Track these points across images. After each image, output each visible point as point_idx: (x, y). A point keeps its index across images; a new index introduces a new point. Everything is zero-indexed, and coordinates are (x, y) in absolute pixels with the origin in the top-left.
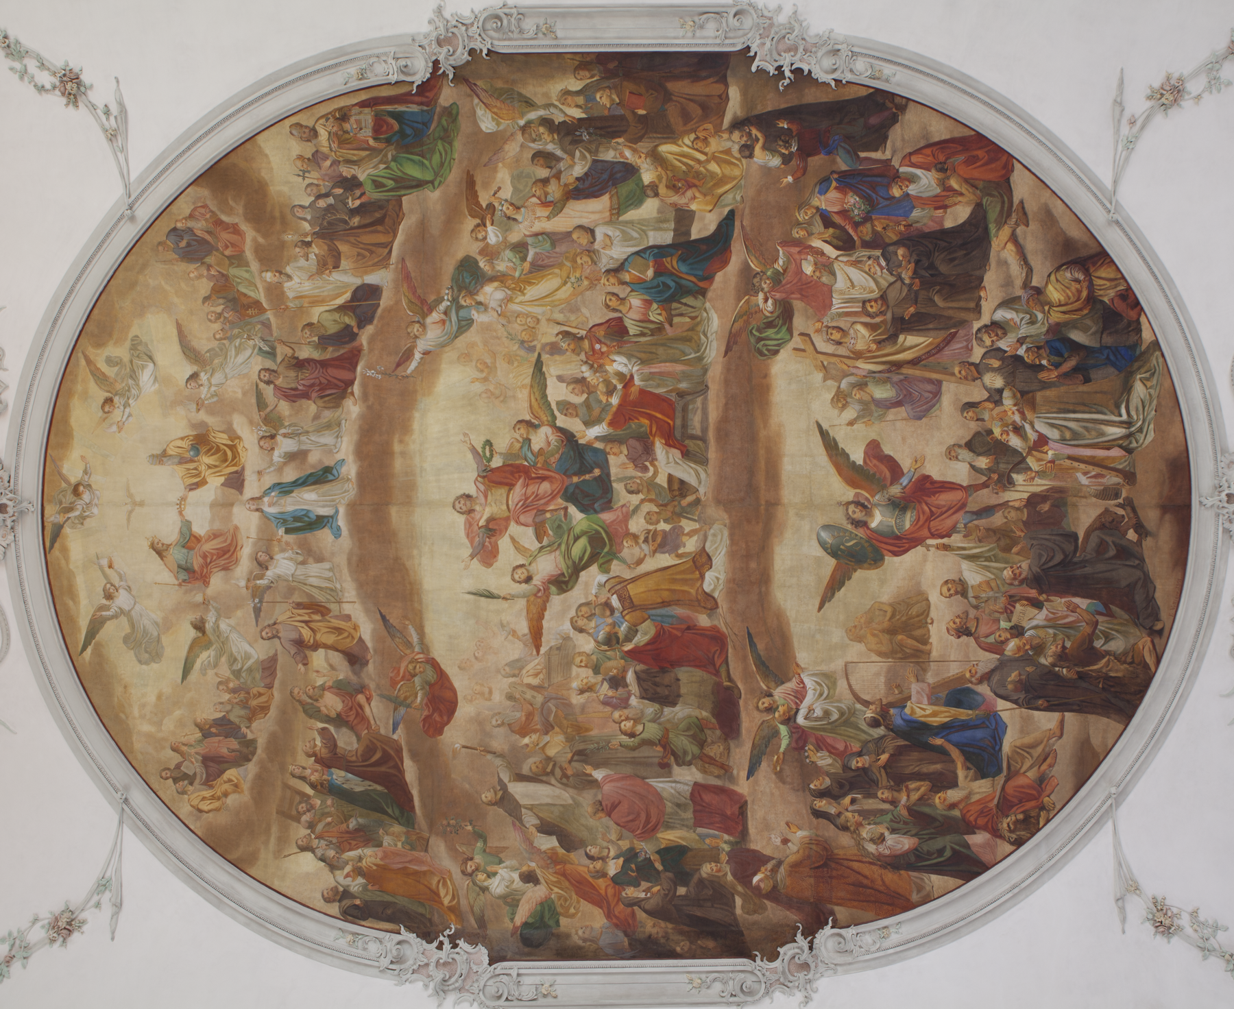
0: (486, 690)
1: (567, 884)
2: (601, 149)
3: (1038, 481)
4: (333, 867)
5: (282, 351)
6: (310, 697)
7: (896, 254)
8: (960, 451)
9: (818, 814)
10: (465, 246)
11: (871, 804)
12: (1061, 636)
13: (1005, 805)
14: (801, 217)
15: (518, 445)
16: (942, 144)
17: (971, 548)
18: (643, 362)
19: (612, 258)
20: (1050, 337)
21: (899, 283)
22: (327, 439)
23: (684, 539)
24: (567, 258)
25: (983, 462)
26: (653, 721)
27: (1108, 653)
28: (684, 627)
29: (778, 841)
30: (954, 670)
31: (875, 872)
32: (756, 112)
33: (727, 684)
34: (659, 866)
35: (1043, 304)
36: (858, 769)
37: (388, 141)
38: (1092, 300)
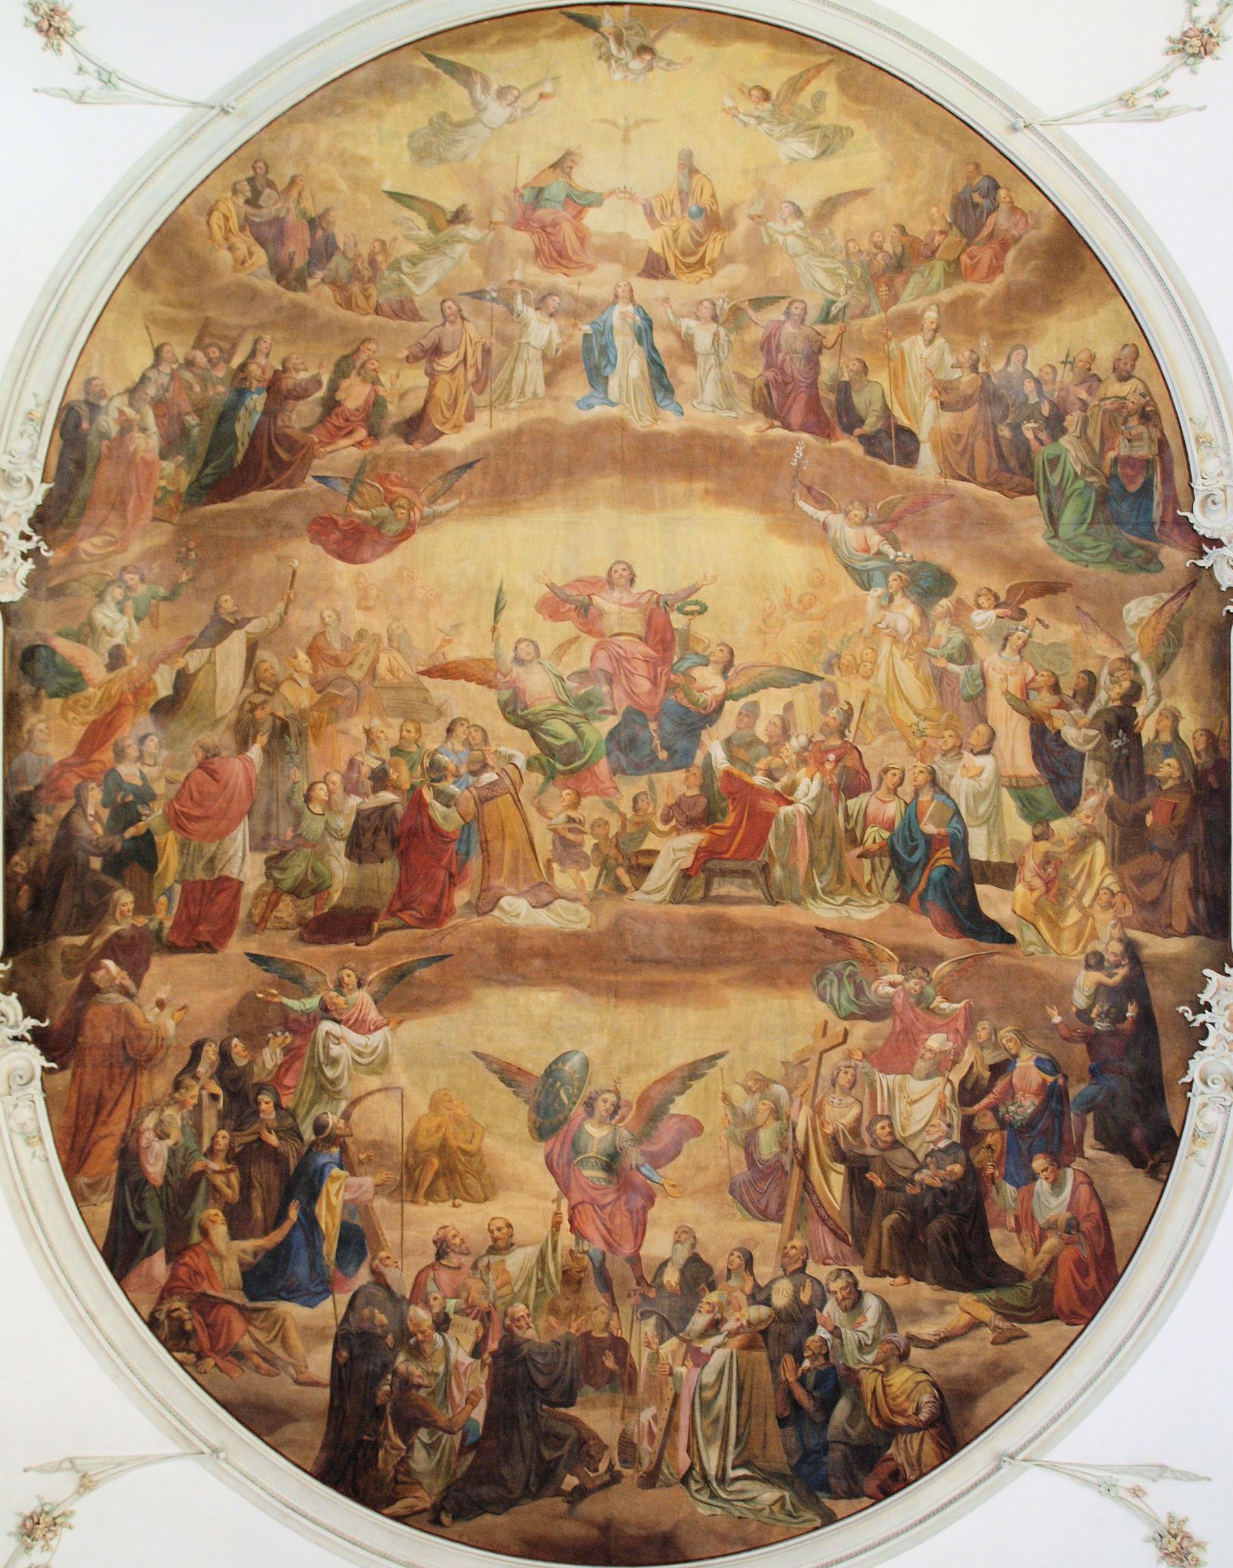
0: (371, 603)
1: (107, 709)
2: (1099, 765)
3: (646, 1352)
4: (133, 392)
5: (831, 332)
6: (363, 366)
7: (955, 1162)
8: (687, 1246)
9: (197, 1048)
10: (971, 580)
11: (210, 1121)
12: (434, 1383)
13: (205, 1304)
14: (1007, 1034)
15: (699, 648)
16: (1104, 1225)
17: (554, 1259)
18: (810, 819)
19: (951, 777)
20: (841, 1372)
21: (913, 1164)
22: (711, 391)
23: (572, 871)
24: (950, 717)
25: (671, 1277)
26: (327, 827)
27: (410, 1448)
28: (454, 870)
29: (162, 995)
30: (390, 1236)
31: (117, 1125)
32: (1147, 972)
33: (376, 926)
34: (131, 832)
35: (884, 1361)
36: (258, 1103)
37: (1112, 477)
38: (892, 1431)
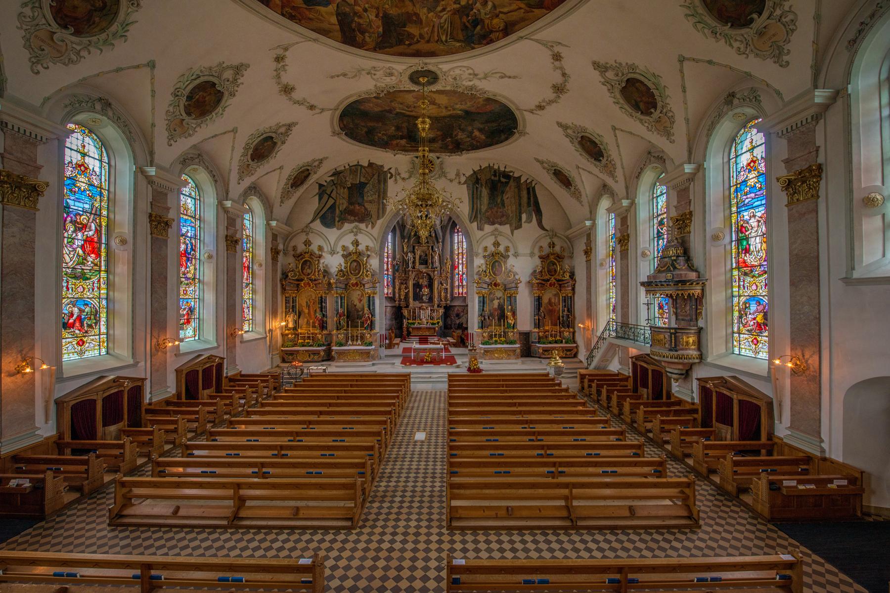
38: (491, 32)
